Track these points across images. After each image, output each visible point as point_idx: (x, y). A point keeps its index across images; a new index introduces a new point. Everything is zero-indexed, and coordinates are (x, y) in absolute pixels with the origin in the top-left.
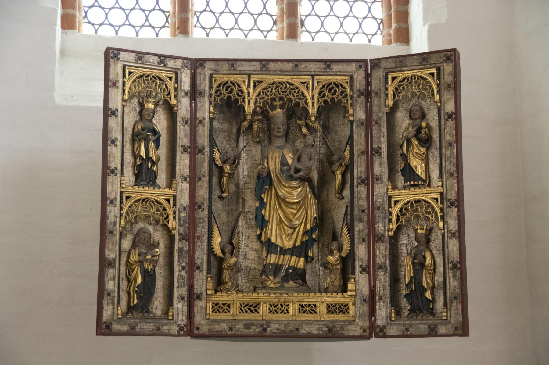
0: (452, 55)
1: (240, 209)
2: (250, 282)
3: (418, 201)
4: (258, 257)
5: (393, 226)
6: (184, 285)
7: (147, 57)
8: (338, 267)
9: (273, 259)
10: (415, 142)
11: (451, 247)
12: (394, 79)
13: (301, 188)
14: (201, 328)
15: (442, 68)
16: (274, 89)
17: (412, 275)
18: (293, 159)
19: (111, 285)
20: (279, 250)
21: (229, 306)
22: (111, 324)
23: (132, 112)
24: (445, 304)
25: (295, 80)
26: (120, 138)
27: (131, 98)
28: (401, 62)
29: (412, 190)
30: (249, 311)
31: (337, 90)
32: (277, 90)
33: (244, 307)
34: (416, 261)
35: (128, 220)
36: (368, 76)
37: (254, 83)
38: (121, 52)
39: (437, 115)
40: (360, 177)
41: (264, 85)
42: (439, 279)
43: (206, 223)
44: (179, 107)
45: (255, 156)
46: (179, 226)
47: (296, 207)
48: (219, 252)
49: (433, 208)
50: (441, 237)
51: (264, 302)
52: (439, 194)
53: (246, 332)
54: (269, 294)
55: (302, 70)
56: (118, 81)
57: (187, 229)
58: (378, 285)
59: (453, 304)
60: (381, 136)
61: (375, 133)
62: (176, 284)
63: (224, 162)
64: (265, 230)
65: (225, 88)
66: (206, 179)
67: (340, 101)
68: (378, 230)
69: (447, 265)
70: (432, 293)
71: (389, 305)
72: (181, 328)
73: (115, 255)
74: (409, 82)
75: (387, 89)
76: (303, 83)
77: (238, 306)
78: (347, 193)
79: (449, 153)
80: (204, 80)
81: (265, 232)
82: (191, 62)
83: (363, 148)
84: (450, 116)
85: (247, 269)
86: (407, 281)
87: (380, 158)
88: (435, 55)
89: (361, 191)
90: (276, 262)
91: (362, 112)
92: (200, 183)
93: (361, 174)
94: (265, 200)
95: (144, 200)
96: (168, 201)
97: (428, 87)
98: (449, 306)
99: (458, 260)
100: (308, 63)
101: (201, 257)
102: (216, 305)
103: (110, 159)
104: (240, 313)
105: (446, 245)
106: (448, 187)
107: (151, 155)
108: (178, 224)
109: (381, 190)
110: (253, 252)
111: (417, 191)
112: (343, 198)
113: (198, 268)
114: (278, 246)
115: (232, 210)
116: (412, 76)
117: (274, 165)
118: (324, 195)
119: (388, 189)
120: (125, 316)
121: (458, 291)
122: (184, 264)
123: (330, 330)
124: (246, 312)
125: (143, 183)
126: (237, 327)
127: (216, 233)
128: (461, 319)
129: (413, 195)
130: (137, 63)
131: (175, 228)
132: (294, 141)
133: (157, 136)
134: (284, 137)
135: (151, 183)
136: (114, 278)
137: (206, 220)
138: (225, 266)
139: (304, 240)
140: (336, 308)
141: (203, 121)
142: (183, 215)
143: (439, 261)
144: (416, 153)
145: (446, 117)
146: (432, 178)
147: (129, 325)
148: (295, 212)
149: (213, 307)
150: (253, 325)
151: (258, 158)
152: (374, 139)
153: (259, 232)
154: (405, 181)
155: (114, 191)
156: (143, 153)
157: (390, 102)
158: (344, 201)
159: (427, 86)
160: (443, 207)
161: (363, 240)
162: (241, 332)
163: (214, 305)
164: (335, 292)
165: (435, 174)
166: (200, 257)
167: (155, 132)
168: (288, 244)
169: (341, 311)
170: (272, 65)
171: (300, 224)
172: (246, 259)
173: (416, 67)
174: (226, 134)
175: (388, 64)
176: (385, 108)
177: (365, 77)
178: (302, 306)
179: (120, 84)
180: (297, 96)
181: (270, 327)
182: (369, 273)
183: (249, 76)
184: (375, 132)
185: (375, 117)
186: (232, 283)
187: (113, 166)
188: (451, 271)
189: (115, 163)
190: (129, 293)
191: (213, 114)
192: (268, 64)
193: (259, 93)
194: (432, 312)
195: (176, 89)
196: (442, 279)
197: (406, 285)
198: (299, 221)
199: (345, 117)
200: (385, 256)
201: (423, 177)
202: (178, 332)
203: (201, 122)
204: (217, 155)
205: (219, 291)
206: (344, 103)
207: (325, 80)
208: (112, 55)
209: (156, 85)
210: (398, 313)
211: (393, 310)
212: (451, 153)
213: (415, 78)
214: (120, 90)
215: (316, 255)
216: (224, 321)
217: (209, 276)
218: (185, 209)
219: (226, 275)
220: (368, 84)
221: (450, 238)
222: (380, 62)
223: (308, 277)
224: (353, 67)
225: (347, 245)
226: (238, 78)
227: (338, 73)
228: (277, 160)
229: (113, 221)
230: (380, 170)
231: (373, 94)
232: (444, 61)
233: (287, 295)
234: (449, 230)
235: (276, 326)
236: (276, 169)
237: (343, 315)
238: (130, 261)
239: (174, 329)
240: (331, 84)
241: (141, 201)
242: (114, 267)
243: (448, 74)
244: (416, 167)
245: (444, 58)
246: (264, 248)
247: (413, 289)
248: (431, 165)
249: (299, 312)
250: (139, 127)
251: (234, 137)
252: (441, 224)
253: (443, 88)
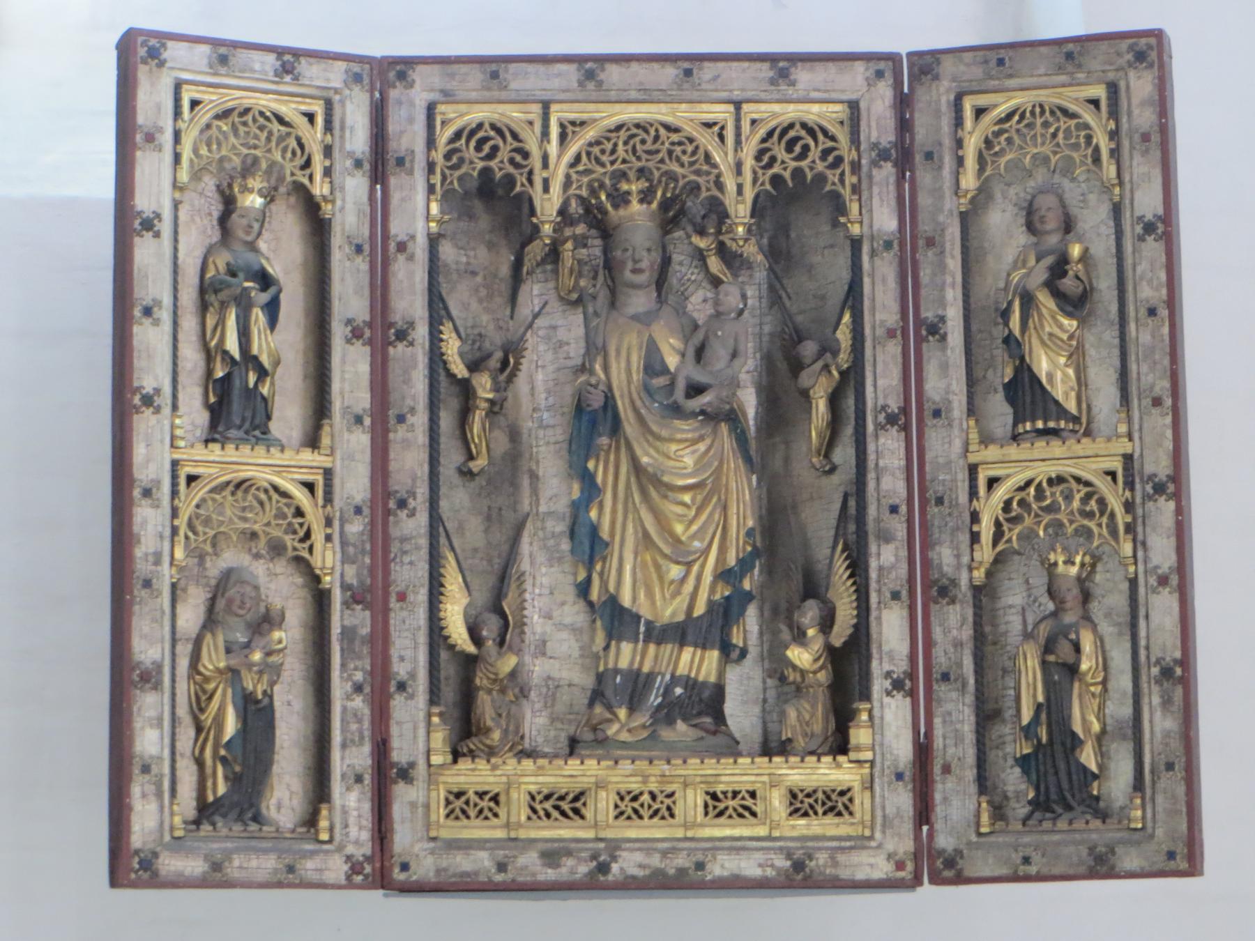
0: (1150, 47)
1: (526, 504)
2: (559, 725)
4: (581, 648)
5: (985, 553)
6: (362, 738)
7: (243, 55)
8: (823, 677)
9: (625, 655)
10: (1046, 301)
12: (980, 112)
13: (708, 441)
14: (413, 866)
15: (1122, 84)
16: (620, 144)
17: (1041, 699)
18: (683, 355)
20: (642, 629)
21: (495, 799)
22: (155, 855)
23: (198, 219)
24: (1138, 785)
25: (682, 115)
27: (196, 176)
28: (1001, 62)
29: (1040, 444)
30: (555, 814)
31: (812, 144)
32: (629, 147)
33: (541, 802)
34: (1051, 658)
35: (193, 545)
36: (903, 103)
37: (562, 126)
38: (170, 44)
39: (1112, 223)
40: (884, 408)
41: (590, 134)
43: (424, 553)
44: (339, 203)
45: (568, 344)
46: (343, 563)
47: (693, 500)
49: (1102, 502)
50: (1125, 586)
52: (1120, 458)
53: (550, 875)
54: (616, 762)
55: (704, 86)
56: (161, 130)
57: (365, 572)
58: (939, 730)
59: (1161, 785)
60: (944, 283)
61: (925, 275)
63: (474, 366)
64: (598, 567)
65: (473, 144)
66: (420, 420)
67: (821, 179)
68: (940, 566)
70: (1102, 754)
72: (355, 868)
73: (159, 650)
74: (1025, 122)
75: (959, 143)
76: (708, 125)
78: (844, 454)
80: (411, 120)
81: (601, 574)
82: (371, 69)
84: (1149, 228)
86: (1027, 716)
87: (944, 349)
88: (1104, 46)
90: (636, 666)
91: (886, 210)
93: (885, 397)
94: (599, 479)
95: (238, 485)
96: (310, 487)
98: (1148, 792)
99: (1178, 654)
100: (721, 65)
102: (459, 795)
103: (139, 363)
104: (529, 818)
105: (1142, 612)
106: (1147, 439)
108: (339, 556)
109: (946, 446)
110: (564, 635)
111: (1056, 448)
112: (833, 469)
113: (402, 686)
114: (637, 618)
115: (500, 509)
116: (1034, 106)
118: (777, 463)
119: (967, 444)
120: (191, 831)
121: (1176, 744)
123: (798, 866)
124: (548, 815)
125: (233, 433)
128: (1184, 827)
129: (1043, 460)
130: (216, 74)
131: (333, 568)
133: (272, 290)
134: (654, 286)
135: (257, 433)
136: (160, 720)
137: (424, 542)
139: (717, 597)
140: (816, 801)
141: (410, 245)
142: (356, 527)
143: (1120, 658)
144: (1051, 335)
145: (1139, 229)
146: (1095, 410)
149: (448, 802)
150: (569, 853)
151: (576, 350)
152: (923, 292)
153: (582, 576)
156: (232, 345)
157: (969, 181)
158: (836, 479)
159: (1078, 137)
160: (1133, 497)
161: (896, 596)
162: (534, 875)
163: (451, 798)
164: (812, 753)
166: (408, 653)
167: (265, 280)
168: (670, 611)
169: (832, 809)
170: (613, 74)
172: (544, 654)
173: (1045, 78)
174: (479, 279)
175: (962, 68)
176: (955, 198)
177: (894, 106)
178: (714, 796)
179: (167, 138)
180: (692, 164)
181: (620, 860)
182: (912, 694)
183: (546, 106)
184: (928, 271)
185: (925, 227)
186: (505, 732)
187: (148, 385)
188: (1155, 689)
190: (200, 762)
192: (603, 70)
193: (578, 159)
194: (1098, 810)
195: (328, 151)
196: (1127, 711)
197: (1022, 728)
198: (702, 540)
199: (835, 224)
200: (958, 644)
201: (1071, 406)
202: (348, 878)
203: (402, 247)
204: (452, 347)
205: (464, 755)
206: (834, 184)
207: (775, 115)
208: (142, 52)
209: (268, 139)
210: (999, 813)
211: (984, 805)
212: (1153, 337)
213: (1043, 112)
216: (481, 844)
217: (436, 710)
219: (486, 705)
220: (904, 125)
222: (938, 62)
223: (730, 707)
226: (513, 114)
227: (814, 95)
228: (634, 358)
230: (942, 384)
231: (918, 158)
232: (1130, 65)
233: (669, 762)
234: (1150, 566)
236: (629, 382)
237: (837, 820)
238: (202, 669)
239: (337, 868)
240: (791, 126)
241: (231, 488)
242: (157, 686)
243: (1143, 104)
244: (1050, 376)
245: (1130, 57)
246: (599, 623)
247: (1044, 740)
249: (706, 814)
251: (505, 288)
252: (1127, 549)
253: (1126, 143)
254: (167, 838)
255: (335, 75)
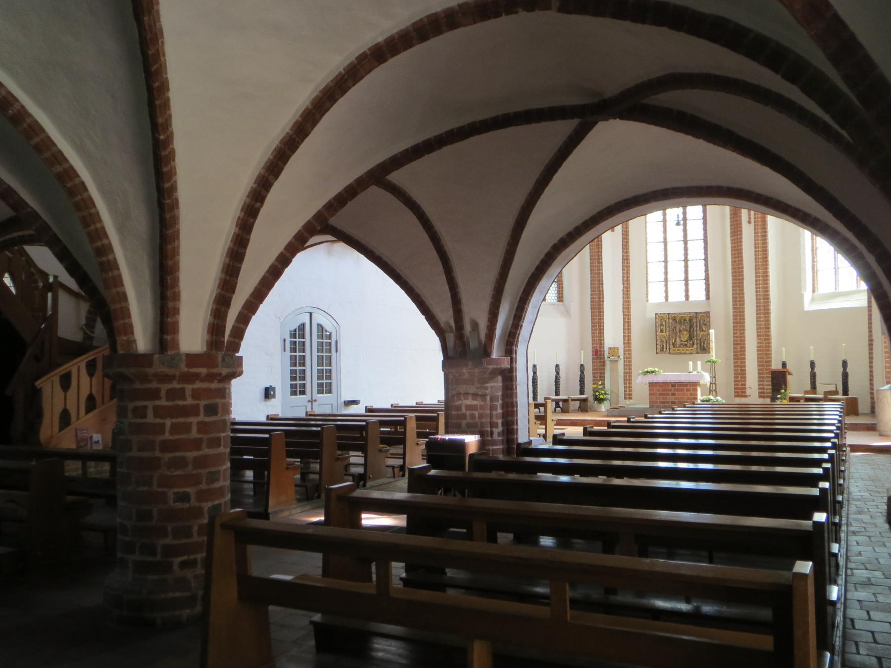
19: (658, 347)
25: (685, 316)
89: (695, 332)
101: (671, 343)
117: (682, 328)
155: (658, 334)
189: (657, 330)
210: (701, 350)
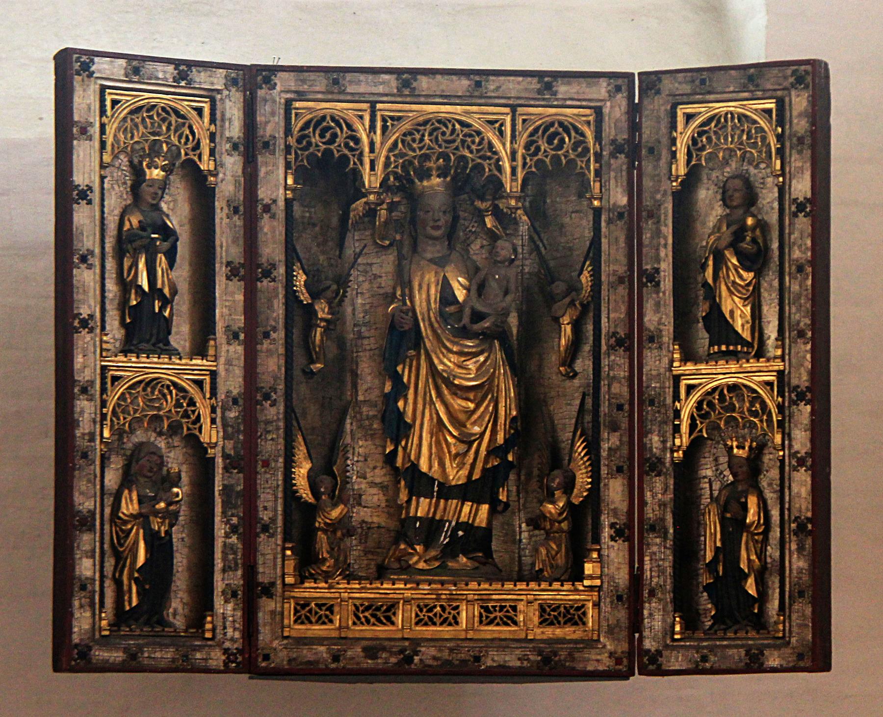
2: (370, 557)
3: (733, 388)
4: (387, 501)
5: (683, 440)
6: (236, 564)
7: (150, 66)
9: (422, 507)
11: (795, 489)
13: (486, 354)
14: (272, 656)
16: (427, 135)
17: (719, 544)
18: (468, 289)
19: (86, 567)
20: (436, 489)
21: (330, 609)
22: (90, 648)
23: (116, 187)
26: (97, 251)
30: (372, 620)
31: (567, 139)
32: (433, 137)
33: (363, 612)
34: (728, 515)
35: (116, 427)
36: (634, 110)
37: (384, 120)
38: (96, 59)
40: (614, 334)
41: (406, 126)
42: (772, 551)
44: (221, 175)
45: (381, 277)
47: (475, 396)
48: (306, 494)
51: (407, 601)
54: (418, 585)
55: (489, 94)
56: (91, 124)
57: (240, 446)
58: (647, 567)
59: (796, 607)
60: (659, 244)
61: (647, 236)
62: (219, 564)
63: (315, 295)
64: (403, 443)
65: (318, 132)
66: (279, 335)
67: (571, 162)
68: (651, 448)
69: (787, 526)
70: (761, 583)
71: (670, 607)
73: (93, 503)
74: (720, 126)
75: (673, 141)
76: (491, 122)
77: (351, 608)
78: (583, 364)
79: (797, 287)
81: (405, 448)
82: (244, 75)
83: (622, 269)
85: (362, 528)
86: (709, 556)
87: (658, 293)
90: (431, 515)
91: (619, 190)
92: (266, 344)
93: (616, 326)
94: (405, 380)
95: (148, 384)
96: (199, 384)
97: (759, 139)
99: (809, 514)
100: (502, 78)
102: (303, 606)
104: (354, 624)
105: (787, 484)
107: (159, 286)
108: (221, 434)
109: (657, 362)
110: (374, 491)
111: (733, 367)
112: (576, 374)
113: (265, 528)
114: (433, 480)
115: (331, 399)
116: (726, 114)
119: (672, 361)
120: (115, 631)
122: (235, 520)
124: (368, 621)
125: (143, 346)
126: (349, 653)
127: (301, 452)
129: (724, 374)
130: (130, 82)
131: (216, 444)
132: (467, 245)
133: (171, 239)
134: (446, 238)
136: (94, 551)
138: (319, 522)
139: (489, 466)
141: (273, 206)
147: (126, 650)
148: (472, 406)
149: (296, 611)
150: (384, 649)
152: (644, 250)
154: (711, 344)
156: (144, 282)
157: (680, 168)
158: (576, 382)
159: (756, 138)
161: (620, 470)
162: (358, 664)
163: (299, 608)
165: (771, 331)
166: (269, 505)
167: (168, 233)
168: (456, 475)
170: (424, 83)
171: (483, 434)
172: (360, 504)
174: (317, 229)
175: (677, 85)
176: (669, 182)
177: (628, 113)
180: (478, 151)
181: (420, 654)
184: (648, 235)
185: (648, 202)
186: (337, 560)
188: (794, 538)
189: (88, 305)
190: (118, 583)
191: (294, 190)
192: (416, 80)
194: (759, 623)
195: (212, 137)
196: (777, 554)
197: (707, 565)
198: (480, 426)
199: (581, 196)
200: (662, 505)
201: (746, 335)
202: (226, 664)
203: (267, 208)
204: (301, 279)
206: (581, 168)
208: (77, 66)
209: (168, 129)
210: (691, 623)
211: (677, 619)
213: (733, 118)
214: (97, 144)
215: (513, 497)
216: (320, 641)
217: (289, 545)
218: (235, 401)
220: (634, 127)
221: (795, 469)
222: (660, 80)
224: (602, 89)
225: (583, 479)
227: (569, 103)
228: (433, 291)
229: (87, 431)
230: (655, 318)
233: (455, 586)
235: (433, 651)
236: (429, 310)
238: (121, 515)
239: (217, 658)
240: (552, 124)
241: (142, 385)
242: (92, 529)
244: (732, 312)
246: (403, 483)
248: (765, 309)
250: (135, 222)
252: (778, 438)
254: (97, 636)
255: (218, 80)
